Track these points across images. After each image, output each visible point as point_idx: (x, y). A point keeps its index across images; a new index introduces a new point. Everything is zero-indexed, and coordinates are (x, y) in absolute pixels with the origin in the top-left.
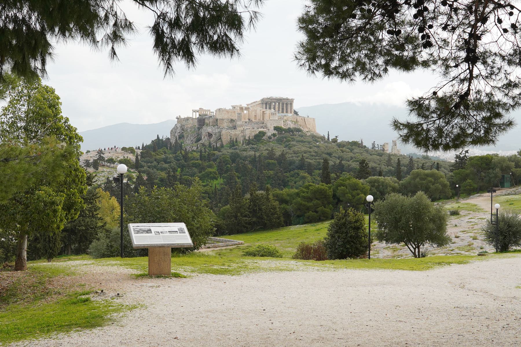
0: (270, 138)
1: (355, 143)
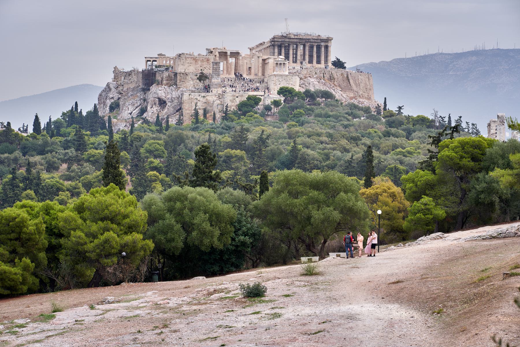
0: (268, 108)
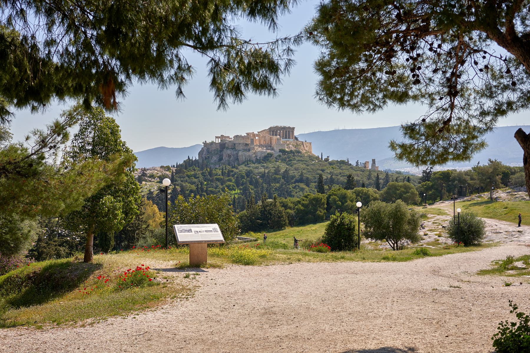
1: (342, 162)
